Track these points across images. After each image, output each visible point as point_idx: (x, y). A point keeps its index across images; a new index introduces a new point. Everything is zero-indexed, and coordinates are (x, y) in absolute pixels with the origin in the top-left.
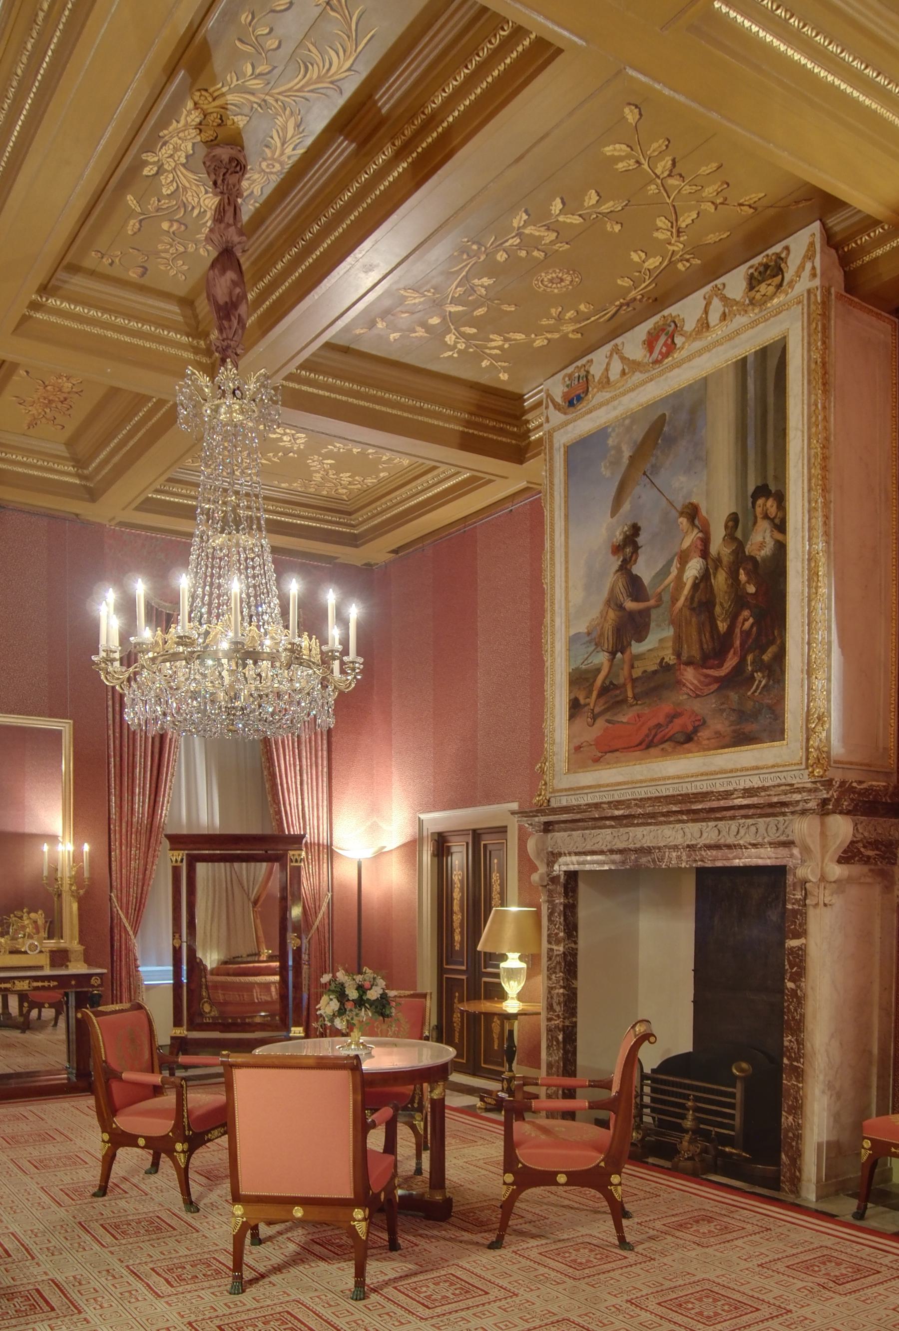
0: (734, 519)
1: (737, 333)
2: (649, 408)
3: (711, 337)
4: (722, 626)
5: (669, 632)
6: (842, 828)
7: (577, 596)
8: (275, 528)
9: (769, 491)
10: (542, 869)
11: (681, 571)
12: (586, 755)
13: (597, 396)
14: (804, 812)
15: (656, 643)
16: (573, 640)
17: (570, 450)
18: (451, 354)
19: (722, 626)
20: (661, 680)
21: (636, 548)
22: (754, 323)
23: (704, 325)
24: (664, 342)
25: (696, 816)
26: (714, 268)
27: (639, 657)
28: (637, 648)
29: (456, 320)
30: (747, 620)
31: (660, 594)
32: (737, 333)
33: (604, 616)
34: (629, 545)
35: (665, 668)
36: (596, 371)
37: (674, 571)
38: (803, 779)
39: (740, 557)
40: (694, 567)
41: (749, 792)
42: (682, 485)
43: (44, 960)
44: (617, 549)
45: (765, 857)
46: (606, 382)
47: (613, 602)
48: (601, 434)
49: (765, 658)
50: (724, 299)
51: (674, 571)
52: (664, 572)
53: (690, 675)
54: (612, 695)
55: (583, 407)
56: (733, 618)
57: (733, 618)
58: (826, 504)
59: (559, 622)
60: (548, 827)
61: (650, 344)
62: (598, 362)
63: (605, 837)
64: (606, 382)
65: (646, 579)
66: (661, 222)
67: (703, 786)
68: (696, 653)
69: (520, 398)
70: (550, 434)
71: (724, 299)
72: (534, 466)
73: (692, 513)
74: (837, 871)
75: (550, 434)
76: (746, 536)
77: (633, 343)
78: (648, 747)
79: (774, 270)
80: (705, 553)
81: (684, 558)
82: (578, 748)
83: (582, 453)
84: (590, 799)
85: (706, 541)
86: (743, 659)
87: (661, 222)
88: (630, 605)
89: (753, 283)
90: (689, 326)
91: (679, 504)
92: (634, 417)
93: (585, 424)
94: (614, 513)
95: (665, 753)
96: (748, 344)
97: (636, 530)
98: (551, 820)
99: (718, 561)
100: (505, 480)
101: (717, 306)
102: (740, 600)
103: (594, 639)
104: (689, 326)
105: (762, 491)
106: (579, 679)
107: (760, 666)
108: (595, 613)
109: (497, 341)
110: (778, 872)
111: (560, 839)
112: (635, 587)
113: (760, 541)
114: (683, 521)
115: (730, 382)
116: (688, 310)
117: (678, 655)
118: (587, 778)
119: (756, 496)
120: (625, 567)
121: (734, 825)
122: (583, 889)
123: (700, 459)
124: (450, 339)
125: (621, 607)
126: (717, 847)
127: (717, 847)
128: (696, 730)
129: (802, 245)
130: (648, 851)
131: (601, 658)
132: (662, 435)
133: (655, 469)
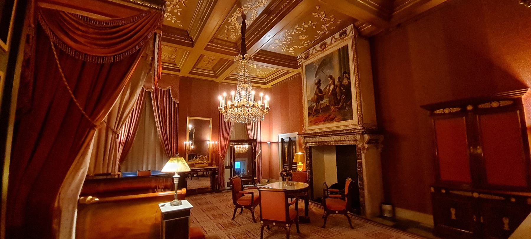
0: (339, 78)
1: (338, 44)
2: (321, 58)
3: (333, 45)
4: (339, 98)
5: (328, 99)
6: (366, 137)
7: (309, 93)
8: (252, 82)
9: (346, 72)
10: (304, 146)
11: (329, 88)
12: (312, 123)
13: (311, 57)
14: (359, 134)
15: (325, 101)
16: (308, 101)
17: (306, 66)
18: (283, 51)
19: (339, 98)
20: (327, 109)
21: (320, 84)
22: (341, 42)
23: (331, 43)
24: (324, 46)
25: (336, 135)
26: (332, 33)
27: (321, 104)
28: (321, 102)
29: (284, 44)
30: (344, 97)
31: (325, 93)
32: (338, 44)
33: (314, 96)
34: (318, 83)
35: (327, 106)
36: (311, 52)
37: (328, 88)
38: (358, 127)
39: (341, 85)
40: (332, 87)
41: (347, 130)
42: (328, 72)
43: (207, 165)
44: (316, 84)
45: (352, 143)
46: (312, 54)
47: (316, 94)
48: (313, 63)
49: (348, 103)
50: (335, 39)
51: (328, 88)
52: (326, 88)
53: (332, 107)
54: (317, 112)
55: (309, 59)
56: (341, 96)
57: (341, 96)
58: (358, 74)
59: (305, 98)
60: (305, 137)
61: (321, 47)
62: (311, 50)
63: (317, 139)
64: (312, 54)
65: (323, 90)
66: (323, 26)
67: (337, 129)
68: (333, 103)
69: (296, 57)
70: (302, 64)
71: (335, 39)
72: (299, 70)
73: (331, 77)
74: (366, 146)
75: (302, 64)
76: (343, 80)
77: (318, 47)
78: (325, 121)
79: (345, 33)
80: (334, 84)
81: (330, 85)
82: (310, 122)
83: (308, 67)
84: (313, 132)
85: (334, 82)
86: (343, 104)
87: (323, 26)
88: (319, 94)
89: (340, 35)
90: (328, 43)
91: (328, 75)
92: (318, 60)
93: (309, 62)
94: (316, 77)
95: (328, 122)
96: (341, 45)
97: (320, 80)
98: (306, 136)
99: (337, 86)
100: (294, 72)
101: (334, 40)
102: (342, 93)
103: (312, 101)
104: (328, 43)
105: (345, 72)
106: (310, 108)
107: (347, 105)
108: (313, 96)
109: (292, 48)
110: (354, 146)
111: (308, 139)
112: (320, 91)
113: (345, 82)
114: (329, 79)
115: (337, 53)
116: (328, 41)
117: (330, 103)
118: (312, 127)
119: (344, 74)
120: (318, 88)
121: (344, 137)
122: (313, 149)
123: (332, 67)
124: (283, 48)
125: (317, 95)
126: (341, 141)
127: (341, 141)
128: (334, 118)
129: (350, 28)
130: (326, 142)
131: (315, 104)
132: (325, 63)
133: (323, 69)
